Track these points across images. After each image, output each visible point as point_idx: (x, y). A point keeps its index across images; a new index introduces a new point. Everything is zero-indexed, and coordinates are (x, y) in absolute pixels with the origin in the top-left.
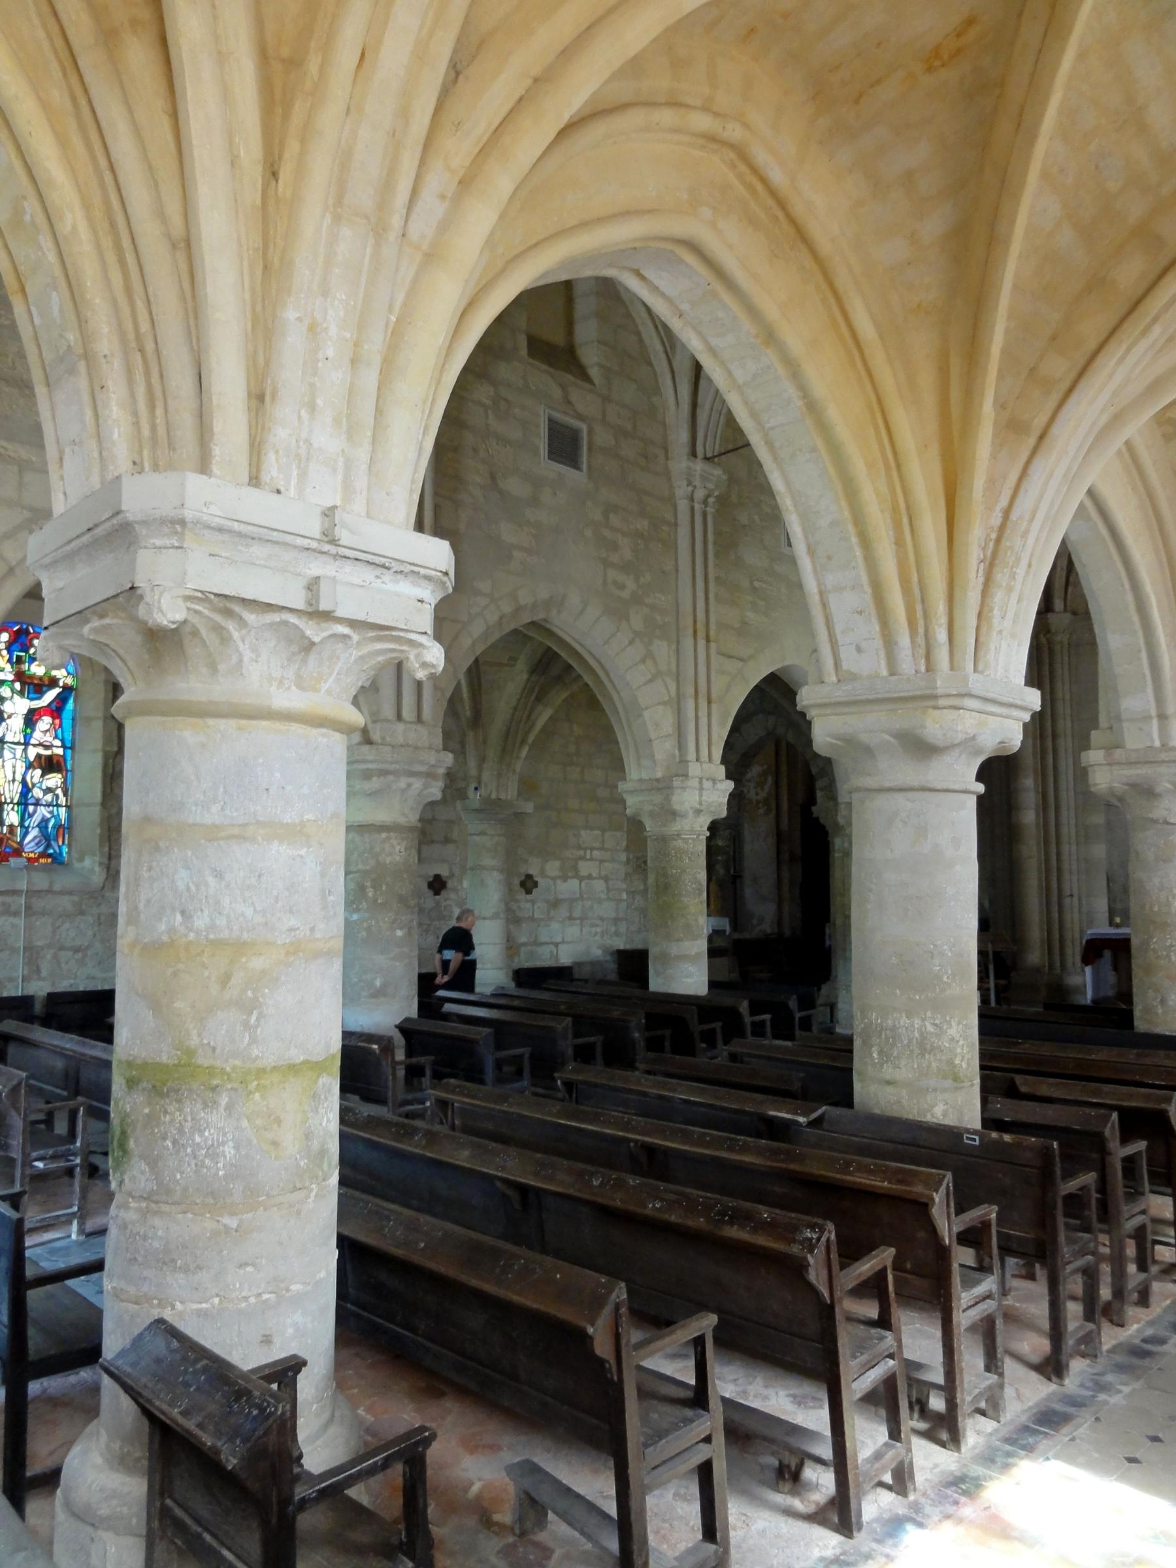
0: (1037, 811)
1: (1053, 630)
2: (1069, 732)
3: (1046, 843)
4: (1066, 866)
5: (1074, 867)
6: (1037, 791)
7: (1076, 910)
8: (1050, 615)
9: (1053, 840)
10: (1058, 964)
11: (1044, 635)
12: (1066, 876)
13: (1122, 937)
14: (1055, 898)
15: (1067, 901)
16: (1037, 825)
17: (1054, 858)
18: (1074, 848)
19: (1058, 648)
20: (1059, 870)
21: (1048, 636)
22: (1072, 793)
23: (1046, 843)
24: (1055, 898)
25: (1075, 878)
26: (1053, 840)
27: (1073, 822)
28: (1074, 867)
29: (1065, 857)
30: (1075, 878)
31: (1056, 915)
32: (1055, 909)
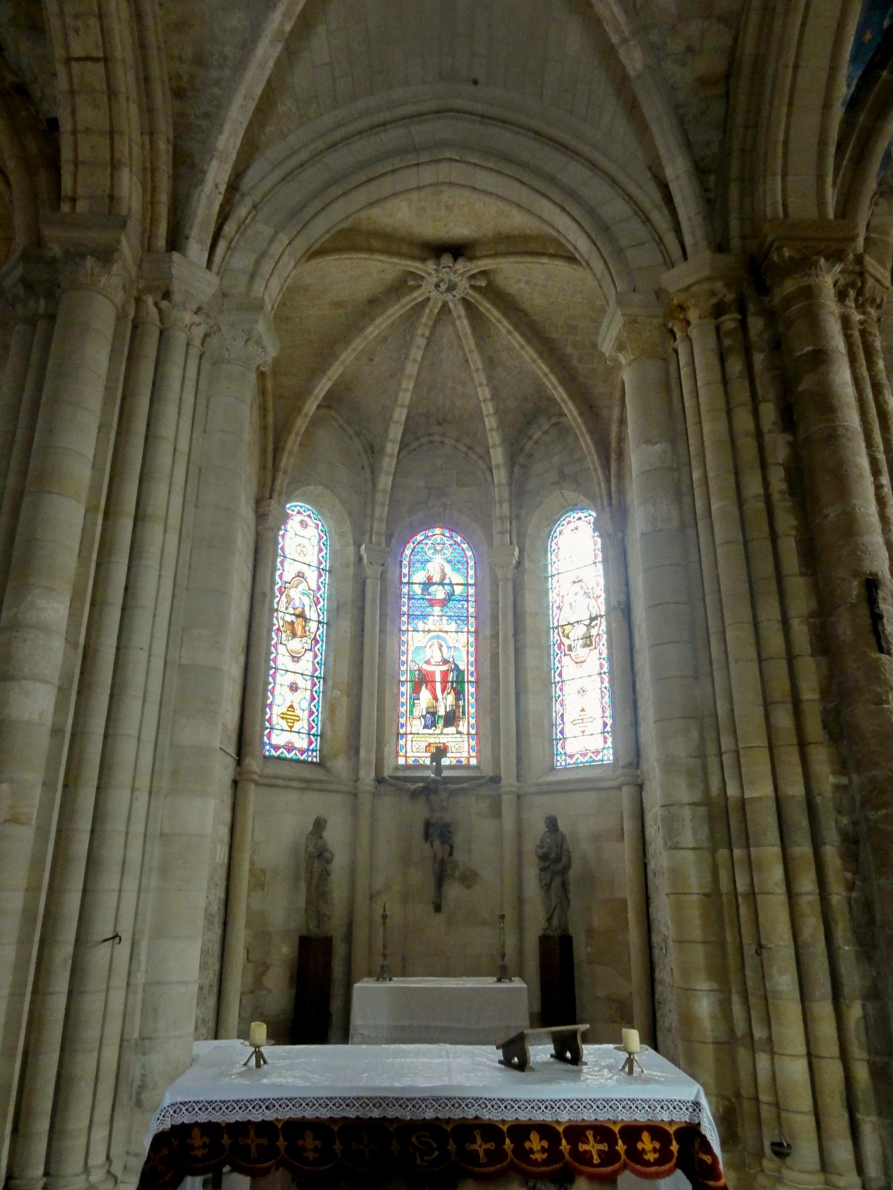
0: (62, 691)
1: (177, 297)
2: (174, 520)
3: (71, 784)
4: (113, 850)
5: (135, 853)
6: (71, 642)
7: (119, 981)
8: (176, 256)
9: (91, 773)
10: (40, 1171)
11: (156, 304)
12: (109, 881)
13: (284, 1114)
14: (65, 950)
15: (100, 955)
16: (56, 731)
17: (84, 826)
18: (141, 805)
19: (179, 337)
20: (93, 862)
21: (164, 304)
22: (158, 664)
23: (71, 784)
24: (65, 950)
25: (131, 885)
26: (91, 773)
27: (149, 734)
28: (135, 853)
29: (116, 824)
30: (131, 885)
31: (58, 1004)
32: (61, 983)
